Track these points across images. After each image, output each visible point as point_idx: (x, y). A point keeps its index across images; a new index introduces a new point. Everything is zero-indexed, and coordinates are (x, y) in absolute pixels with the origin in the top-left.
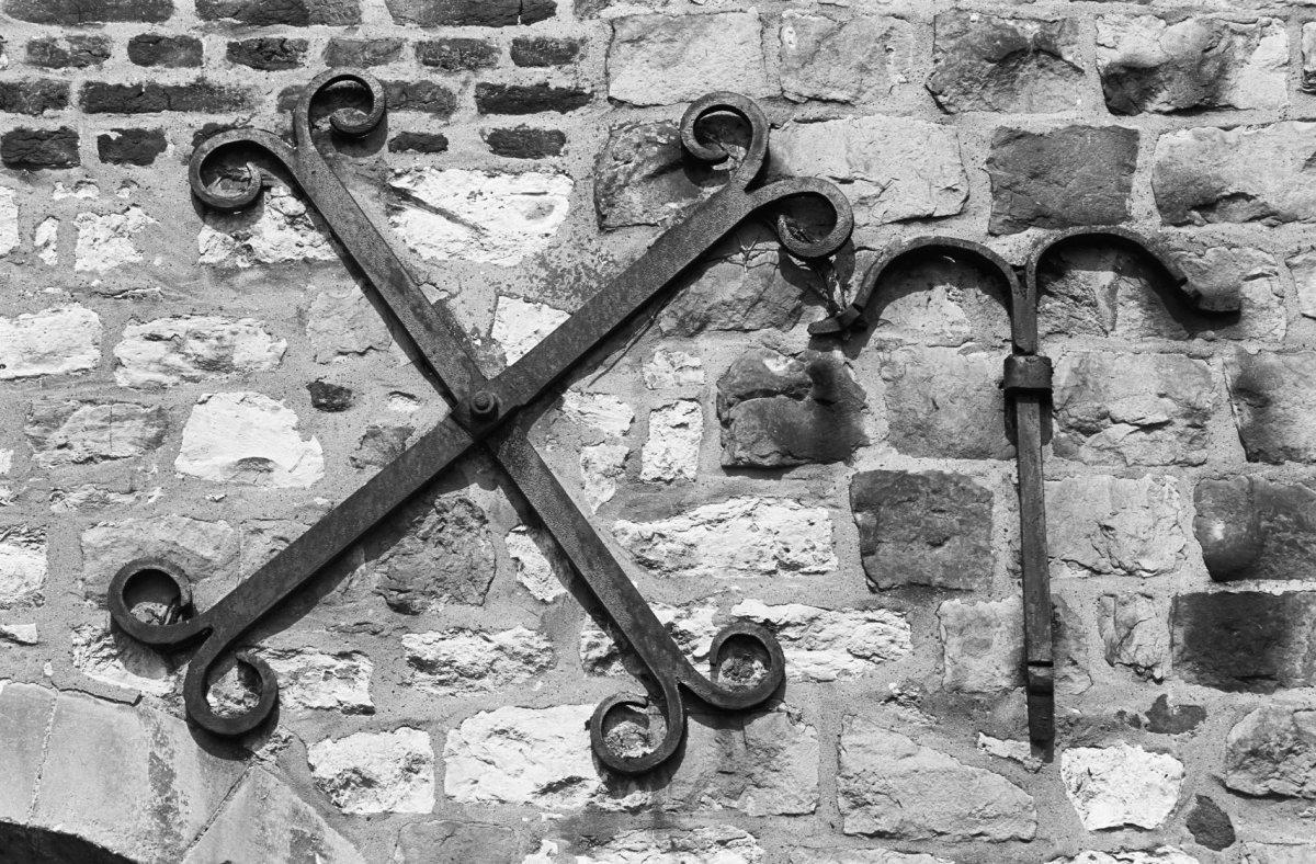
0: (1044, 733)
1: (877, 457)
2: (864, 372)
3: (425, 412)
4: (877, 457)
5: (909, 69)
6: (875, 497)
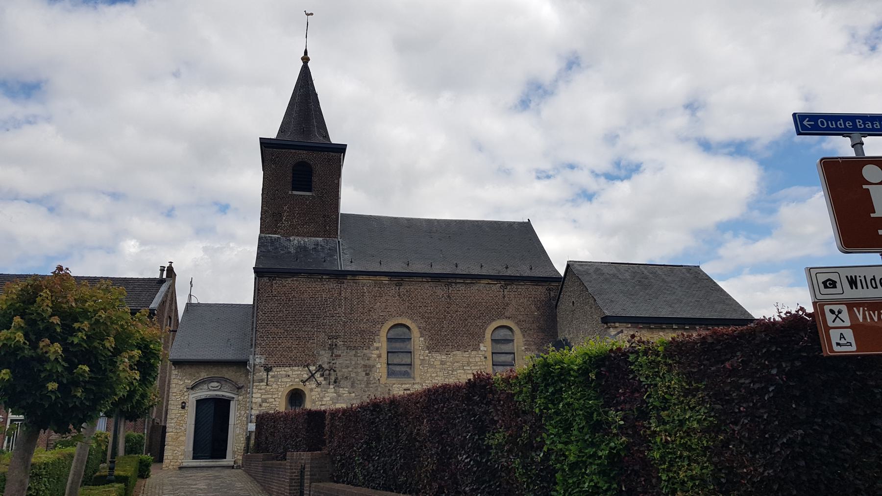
0: (329, 385)
1: (325, 376)
2: (324, 373)
3: (310, 375)
4: (325, 376)
5: (327, 363)
6: (325, 378)
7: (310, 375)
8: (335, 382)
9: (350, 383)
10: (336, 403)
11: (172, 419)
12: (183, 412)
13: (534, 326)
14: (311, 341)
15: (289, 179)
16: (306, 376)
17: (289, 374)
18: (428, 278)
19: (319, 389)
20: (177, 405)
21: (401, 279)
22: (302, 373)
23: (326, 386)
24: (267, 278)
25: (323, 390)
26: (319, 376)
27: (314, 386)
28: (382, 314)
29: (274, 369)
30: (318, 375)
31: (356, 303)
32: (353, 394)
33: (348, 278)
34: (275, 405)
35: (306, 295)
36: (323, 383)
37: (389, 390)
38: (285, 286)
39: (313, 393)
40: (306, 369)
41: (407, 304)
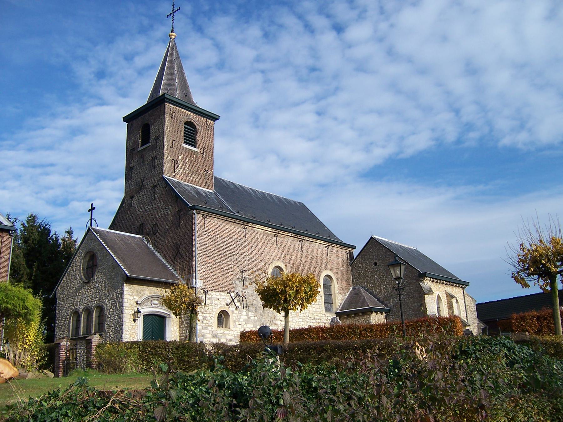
7: (232, 300)
8: (246, 307)
9: (254, 309)
10: (248, 323)
11: (127, 331)
12: (134, 324)
13: (342, 277)
14: (230, 273)
15: (182, 133)
16: (229, 301)
17: (219, 298)
18: (292, 234)
19: (237, 312)
20: (129, 318)
21: (278, 232)
22: (227, 298)
23: (241, 309)
24: (202, 215)
25: (240, 313)
26: (237, 301)
27: (234, 309)
28: (268, 257)
29: (209, 293)
30: (236, 301)
31: (254, 246)
32: (256, 318)
33: (250, 225)
34: (212, 322)
35: (225, 235)
36: (240, 307)
37: (275, 316)
38: (212, 224)
39: (234, 315)
40: (229, 294)
41: (281, 251)
